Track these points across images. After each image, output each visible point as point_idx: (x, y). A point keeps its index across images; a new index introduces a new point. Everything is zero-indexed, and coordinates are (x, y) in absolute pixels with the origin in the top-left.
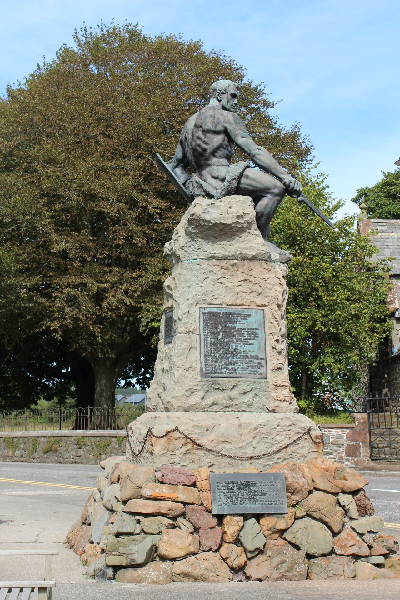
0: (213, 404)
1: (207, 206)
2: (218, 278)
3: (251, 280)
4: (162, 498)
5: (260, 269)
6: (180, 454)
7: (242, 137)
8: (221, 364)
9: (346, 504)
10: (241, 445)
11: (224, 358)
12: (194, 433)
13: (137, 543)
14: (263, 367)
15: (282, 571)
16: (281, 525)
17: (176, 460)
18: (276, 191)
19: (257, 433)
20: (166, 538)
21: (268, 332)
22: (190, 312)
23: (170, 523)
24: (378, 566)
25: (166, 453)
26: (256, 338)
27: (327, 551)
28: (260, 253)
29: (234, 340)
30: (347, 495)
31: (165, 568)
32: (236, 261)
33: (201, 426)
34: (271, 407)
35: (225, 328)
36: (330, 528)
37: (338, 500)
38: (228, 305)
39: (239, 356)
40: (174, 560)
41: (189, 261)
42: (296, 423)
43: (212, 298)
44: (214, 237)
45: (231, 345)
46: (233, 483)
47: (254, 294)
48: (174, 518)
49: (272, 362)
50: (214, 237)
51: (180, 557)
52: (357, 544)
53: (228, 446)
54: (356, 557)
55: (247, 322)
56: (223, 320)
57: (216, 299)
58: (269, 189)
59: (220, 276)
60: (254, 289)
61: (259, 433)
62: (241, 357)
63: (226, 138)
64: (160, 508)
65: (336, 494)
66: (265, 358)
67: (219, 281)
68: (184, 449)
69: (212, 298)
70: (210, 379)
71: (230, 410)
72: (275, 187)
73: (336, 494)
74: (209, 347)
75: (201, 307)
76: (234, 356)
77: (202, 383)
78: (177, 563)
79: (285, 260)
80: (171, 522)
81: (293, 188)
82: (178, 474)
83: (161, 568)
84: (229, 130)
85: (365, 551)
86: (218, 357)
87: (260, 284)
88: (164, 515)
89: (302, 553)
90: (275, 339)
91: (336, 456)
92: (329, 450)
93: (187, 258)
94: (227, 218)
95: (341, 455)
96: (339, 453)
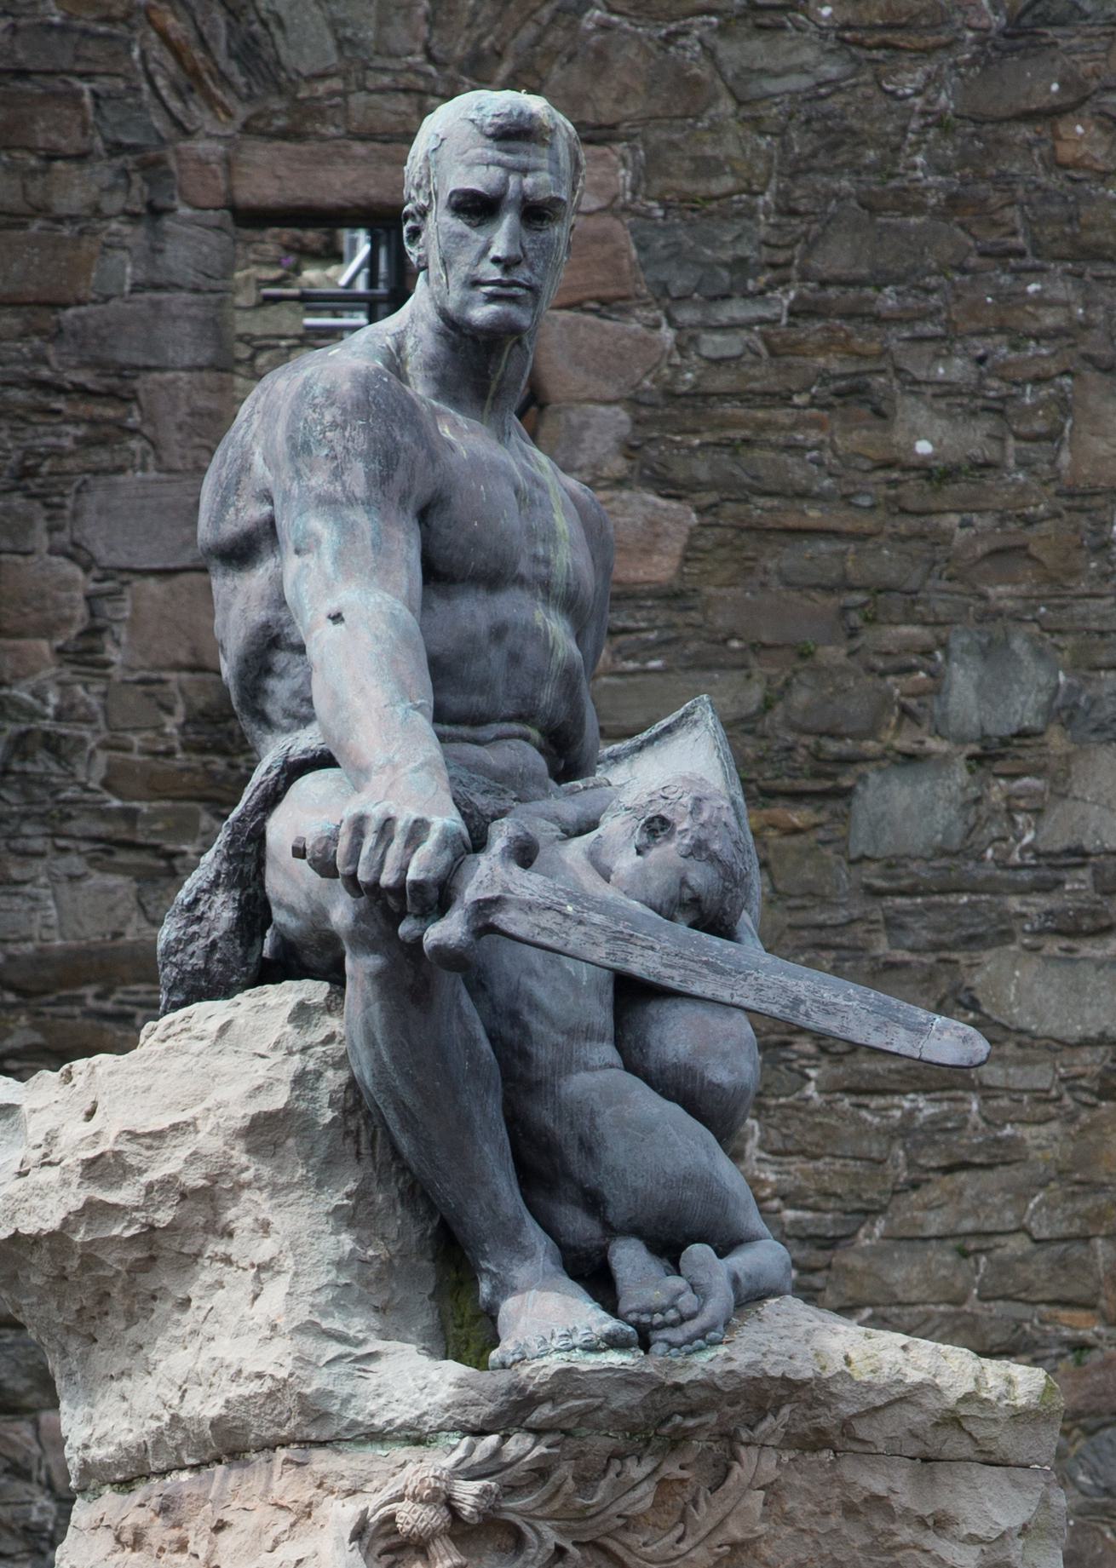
28: (246, 1400)
79: (489, 1409)
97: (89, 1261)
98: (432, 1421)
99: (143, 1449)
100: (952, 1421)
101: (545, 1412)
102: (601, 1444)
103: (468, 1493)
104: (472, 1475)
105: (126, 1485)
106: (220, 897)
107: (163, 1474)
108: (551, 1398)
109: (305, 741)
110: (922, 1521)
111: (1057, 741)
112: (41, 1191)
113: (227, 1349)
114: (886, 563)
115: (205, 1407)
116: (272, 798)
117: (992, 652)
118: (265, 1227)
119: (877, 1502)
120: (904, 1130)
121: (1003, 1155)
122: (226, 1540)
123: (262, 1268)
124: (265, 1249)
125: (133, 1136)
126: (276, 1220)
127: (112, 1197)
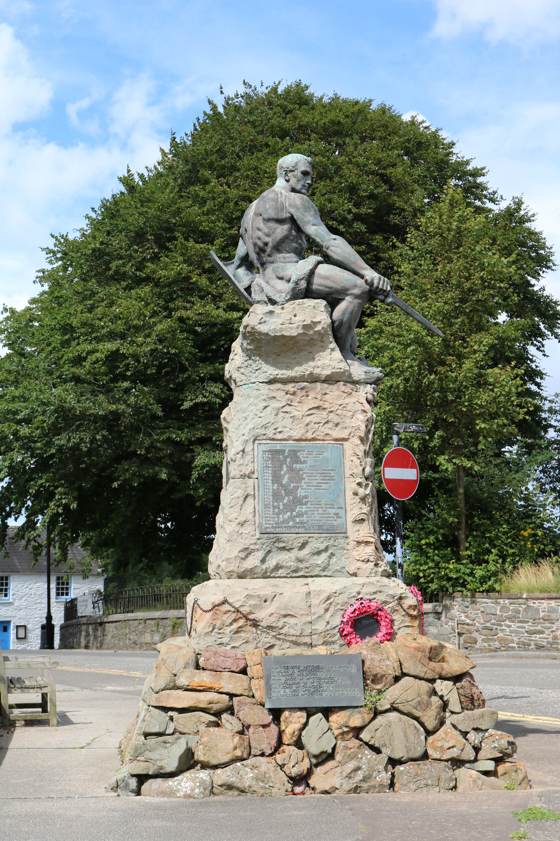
0: (278, 567)
1: (264, 314)
2: (282, 405)
3: (325, 406)
4: (202, 688)
5: (337, 393)
6: (230, 632)
7: (314, 225)
8: (286, 516)
9: (445, 693)
10: (309, 619)
11: (289, 507)
12: (248, 605)
13: (168, 745)
14: (341, 517)
15: (354, 781)
16: (356, 721)
17: (225, 640)
18: (356, 291)
19: (331, 604)
20: (205, 739)
21: (348, 473)
22: (246, 450)
23: (211, 720)
24: (486, 773)
25: (212, 631)
28: (336, 372)
29: (303, 484)
30: (446, 682)
31: (202, 778)
32: (305, 383)
33: (259, 596)
34: (352, 570)
35: (291, 469)
36: (422, 724)
37: (434, 689)
38: (295, 440)
39: (309, 505)
40: (215, 767)
41: (247, 386)
42: (382, 589)
43: (274, 431)
44: (276, 353)
45: (298, 492)
46: (293, 668)
47: (330, 425)
48: (218, 714)
49: (352, 512)
50: (276, 353)
51: (223, 764)
52: (458, 745)
53: (292, 621)
54: (457, 763)
56: (288, 460)
57: (280, 432)
58: (347, 290)
59: (284, 404)
60: (329, 418)
61: (334, 604)
62: (312, 506)
63: (293, 227)
64: (199, 702)
65: (432, 681)
66: (343, 506)
67: (284, 410)
68: (235, 626)
69: (274, 431)
70: (272, 536)
71: (299, 574)
72: (355, 286)
73: (432, 681)
74: (271, 494)
75: (260, 444)
76: (302, 504)
77: (261, 541)
78: (219, 771)
80: (213, 718)
81: (378, 287)
82: (222, 658)
83: (197, 777)
84: (295, 217)
85: (470, 754)
86: (281, 507)
87: (337, 412)
88: (203, 710)
89: (383, 758)
90: (357, 482)
91: (549, 635)
92: (539, 628)
93: (244, 382)
94: (291, 328)
95: (555, 633)
96: (553, 631)
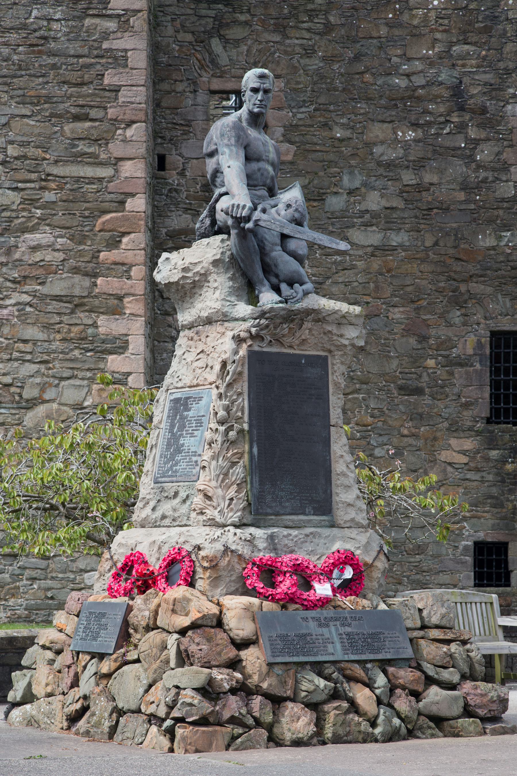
0: (164, 517)
26: (201, 428)
27: (133, 707)
28: (212, 313)
55: (198, 407)
79: (257, 314)
89: (110, 706)
97: (183, 287)
98: (247, 317)
99: (193, 322)
100: (344, 317)
101: (268, 315)
102: (278, 321)
103: (253, 330)
104: (254, 327)
105: (190, 329)
106: (207, 219)
107: (197, 326)
108: (269, 312)
109: (223, 190)
110: (338, 335)
111: (363, 190)
112: (174, 274)
113: (208, 303)
114: (331, 157)
115: (205, 314)
116: (217, 201)
117: (351, 173)
118: (216, 281)
119: (330, 332)
120: (335, 263)
121: (353, 267)
122: (208, 339)
123: (215, 288)
124: (216, 285)
125: (191, 263)
126: (218, 279)
127: (187, 275)
